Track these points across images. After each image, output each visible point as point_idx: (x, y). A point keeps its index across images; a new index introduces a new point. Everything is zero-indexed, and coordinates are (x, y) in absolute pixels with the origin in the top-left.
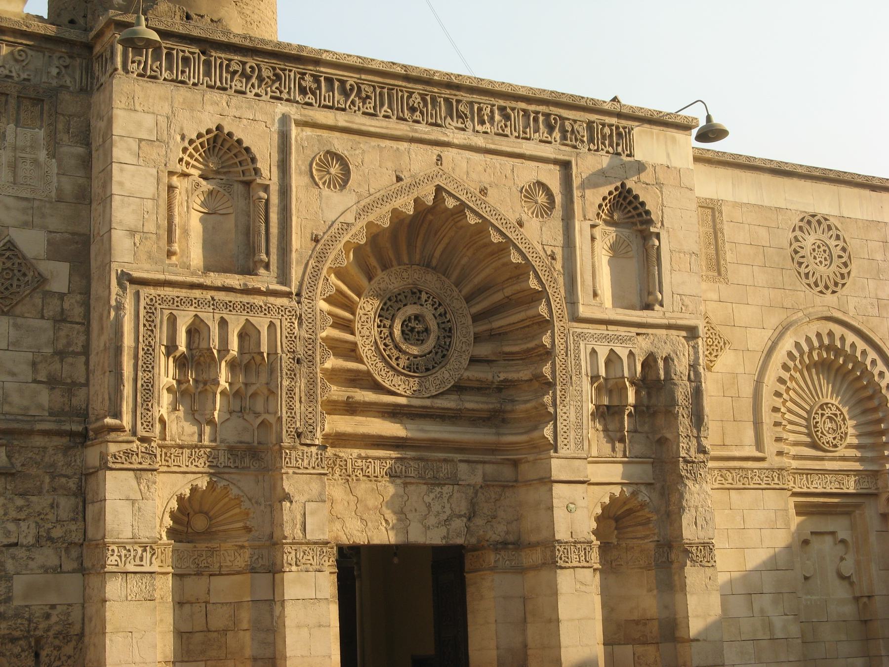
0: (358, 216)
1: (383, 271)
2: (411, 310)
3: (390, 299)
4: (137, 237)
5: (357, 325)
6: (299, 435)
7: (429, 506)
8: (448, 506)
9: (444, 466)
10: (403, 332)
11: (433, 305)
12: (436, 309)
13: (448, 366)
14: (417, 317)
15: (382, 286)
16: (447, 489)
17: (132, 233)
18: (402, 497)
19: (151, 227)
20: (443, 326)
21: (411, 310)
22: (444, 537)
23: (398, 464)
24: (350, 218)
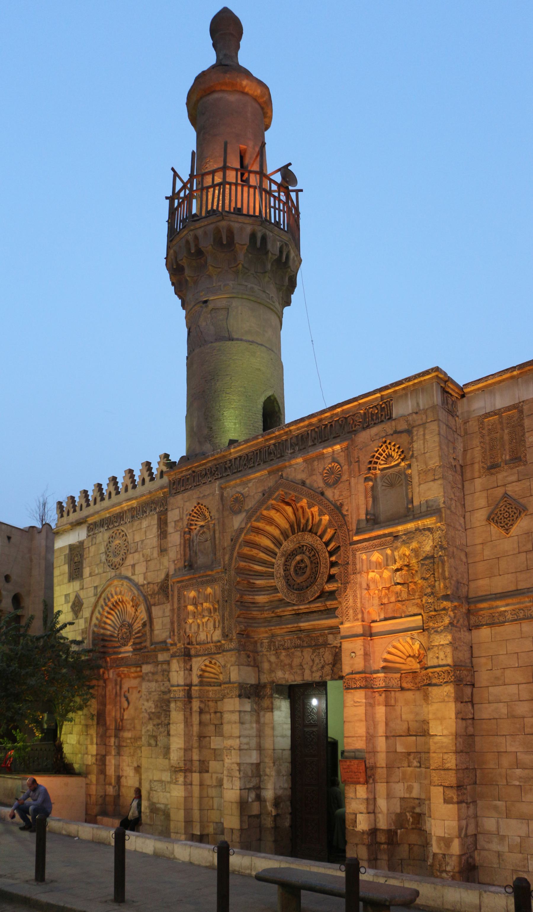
0: (246, 524)
1: (285, 540)
2: (298, 558)
3: (290, 555)
4: (176, 562)
5: (275, 573)
6: (227, 636)
7: (313, 661)
8: (322, 661)
9: (320, 638)
10: (295, 571)
11: (309, 552)
12: (310, 553)
13: (316, 583)
14: (302, 561)
15: (285, 549)
16: (321, 650)
17: (174, 561)
18: (301, 657)
19: (179, 556)
20: (314, 561)
21: (298, 558)
22: (321, 676)
23: (299, 641)
24: (243, 525)
